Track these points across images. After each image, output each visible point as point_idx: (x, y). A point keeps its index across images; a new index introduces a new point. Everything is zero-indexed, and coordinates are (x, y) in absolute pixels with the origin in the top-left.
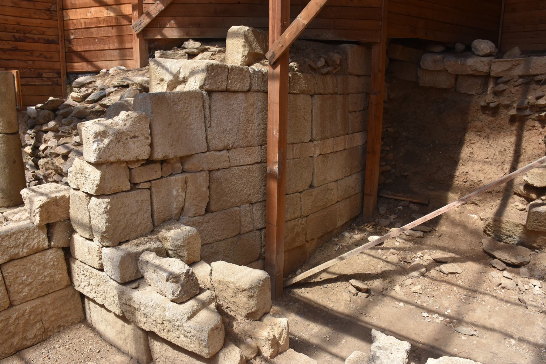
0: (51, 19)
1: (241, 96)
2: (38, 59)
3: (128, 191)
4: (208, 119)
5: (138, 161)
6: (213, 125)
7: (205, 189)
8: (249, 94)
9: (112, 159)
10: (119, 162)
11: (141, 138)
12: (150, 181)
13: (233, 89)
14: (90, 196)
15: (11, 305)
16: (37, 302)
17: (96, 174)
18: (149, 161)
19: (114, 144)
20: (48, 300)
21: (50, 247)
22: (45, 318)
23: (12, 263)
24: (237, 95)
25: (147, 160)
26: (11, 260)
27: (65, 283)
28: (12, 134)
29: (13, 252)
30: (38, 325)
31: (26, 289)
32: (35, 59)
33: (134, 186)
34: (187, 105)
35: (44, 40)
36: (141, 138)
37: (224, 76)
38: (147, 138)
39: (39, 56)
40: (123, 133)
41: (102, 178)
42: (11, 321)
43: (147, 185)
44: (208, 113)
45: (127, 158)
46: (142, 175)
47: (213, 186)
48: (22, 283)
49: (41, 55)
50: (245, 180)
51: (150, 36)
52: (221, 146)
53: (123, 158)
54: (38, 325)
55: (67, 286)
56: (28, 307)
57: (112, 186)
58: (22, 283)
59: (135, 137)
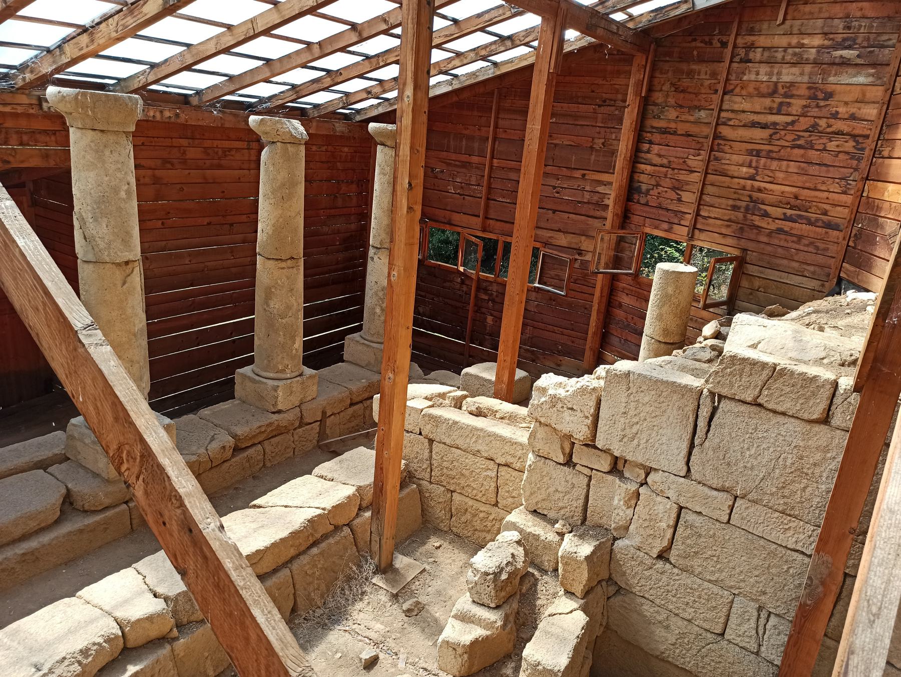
1: (792, 425)
2: (806, 249)
3: (560, 464)
4: (700, 432)
6: (707, 443)
7: (663, 525)
8: (817, 428)
12: (592, 469)
13: (770, 406)
15: (496, 505)
19: (548, 406)
23: (506, 468)
24: (781, 419)
26: (506, 465)
28: (665, 343)
29: (510, 460)
31: (510, 500)
32: (802, 248)
33: (569, 462)
34: (662, 400)
35: (823, 222)
37: (759, 379)
38: (587, 417)
39: (808, 245)
40: (559, 398)
42: (491, 518)
43: (587, 471)
44: (702, 424)
47: (680, 530)
48: (508, 492)
49: (811, 243)
50: (756, 561)
52: (715, 483)
58: (508, 492)
59: (572, 409)
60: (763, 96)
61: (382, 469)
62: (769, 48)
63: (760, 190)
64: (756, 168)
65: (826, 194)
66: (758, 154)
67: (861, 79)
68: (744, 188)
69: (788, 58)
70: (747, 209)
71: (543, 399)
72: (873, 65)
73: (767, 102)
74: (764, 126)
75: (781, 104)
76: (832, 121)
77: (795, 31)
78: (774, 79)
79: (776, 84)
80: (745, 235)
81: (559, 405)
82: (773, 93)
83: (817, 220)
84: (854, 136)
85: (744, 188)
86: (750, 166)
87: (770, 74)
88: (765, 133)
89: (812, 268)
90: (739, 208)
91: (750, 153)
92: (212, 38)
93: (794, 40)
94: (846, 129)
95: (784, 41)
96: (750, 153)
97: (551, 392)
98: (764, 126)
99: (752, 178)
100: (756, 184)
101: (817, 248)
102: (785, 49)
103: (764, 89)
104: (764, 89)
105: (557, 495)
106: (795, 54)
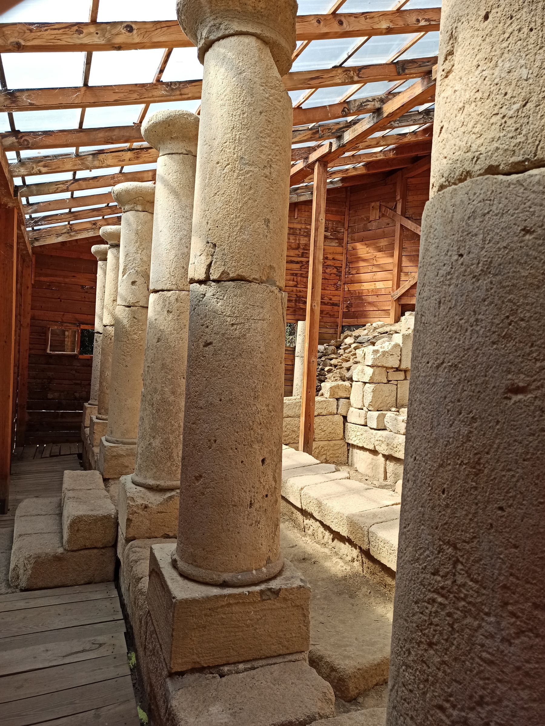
0: (337, 290)
5: (392, 368)
9: (379, 364)
10: (383, 367)
11: (395, 356)
14: (365, 383)
16: (326, 443)
17: (370, 371)
18: (398, 369)
20: (332, 443)
21: (337, 414)
22: (328, 454)
25: (397, 368)
27: (341, 436)
30: (324, 457)
31: (323, 433)
36: (395, 356)
41: (374, 373)
43: (396, 383)
45: (386, 365)
46: (393, 376)
51: (403, 302)
53: (385, 365)
54: (324, 457)
55: (342, 439)
56: (322, 443)
57: (377, 378)
60: (294, 249)
61: (309, 415)
62: (293, 228)
63: (300, 292)
64: (297, 282)
65: (329, 292)
66: (296, 275)
67: (334, 244)
68: (292, 291)
69: (302, 233)
70: (296, 301)
71: (378, 355)
72: (337, 239)
73: (297, 252)
74: (297, 263)
75: (303, 253)
76: (326, 261)
77: (303, 222)
78: (297, 242)
79: (299, 244)
80: (297, 313)
81: (386, 355)
82: (298, 248)
83: (328, 303)
84: (336, 267)
85: (292, 291)
86: (293, 281)
87: (295, 240)
88: (298, 266)
89: (329, 324)
90: (292, 301)
91: (292, 274)
92: (148, 171)
93: (303, 226)
94: (332, 264)
95: (298, 226)
96: (292, 274)
97: (381, 350)
98: (297, 263)
99: (296, 286)
100: (298, 289)
101: (330, 315)
102: (300, 230)
103: (293, 246)
104: (293, 246)
105: (386, 398)
106: (305, 232)
